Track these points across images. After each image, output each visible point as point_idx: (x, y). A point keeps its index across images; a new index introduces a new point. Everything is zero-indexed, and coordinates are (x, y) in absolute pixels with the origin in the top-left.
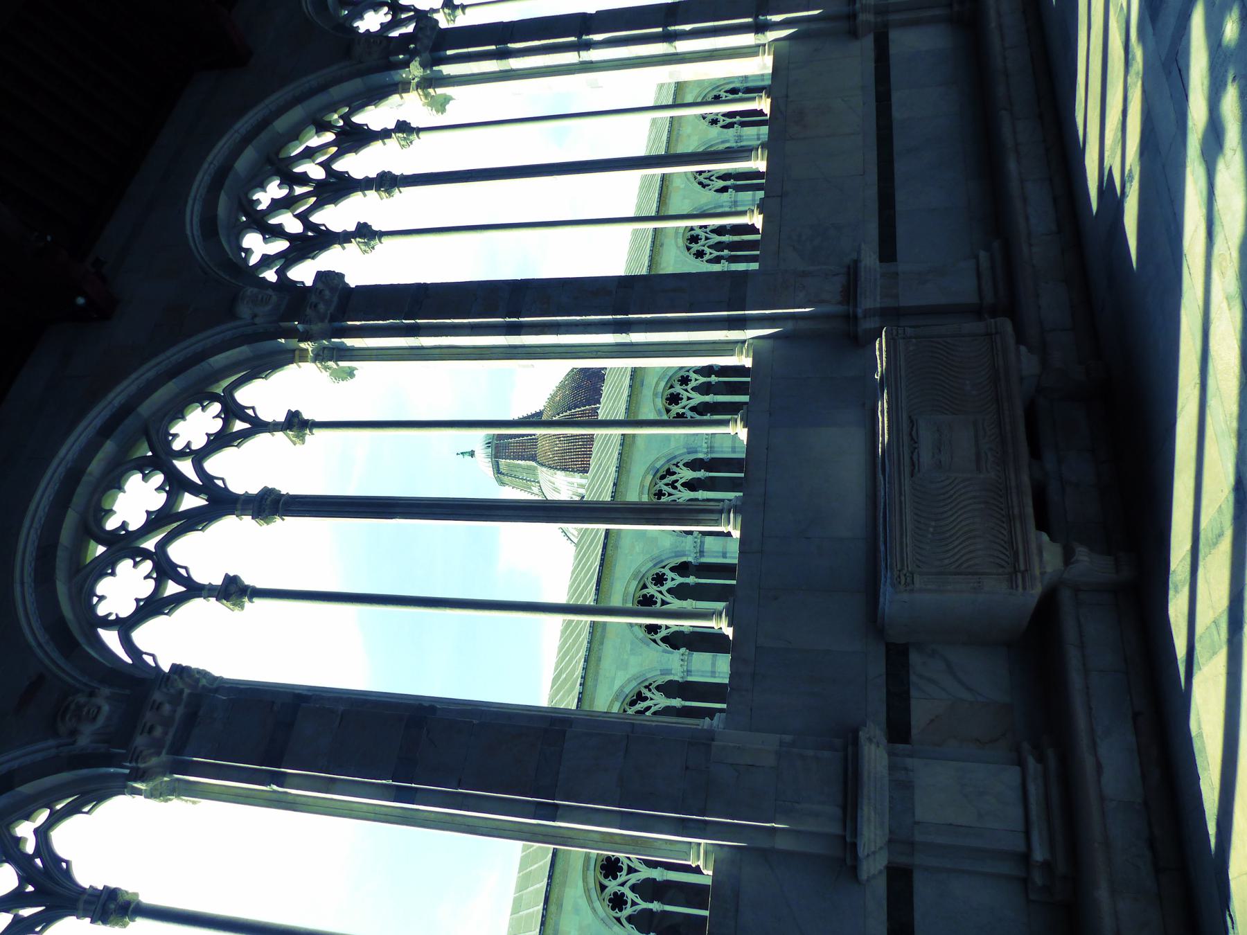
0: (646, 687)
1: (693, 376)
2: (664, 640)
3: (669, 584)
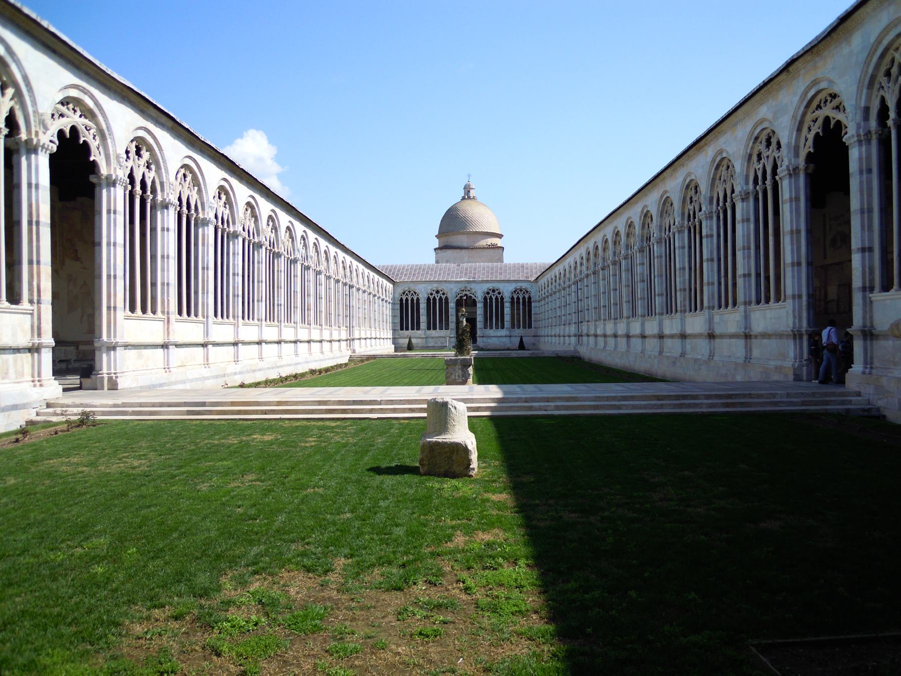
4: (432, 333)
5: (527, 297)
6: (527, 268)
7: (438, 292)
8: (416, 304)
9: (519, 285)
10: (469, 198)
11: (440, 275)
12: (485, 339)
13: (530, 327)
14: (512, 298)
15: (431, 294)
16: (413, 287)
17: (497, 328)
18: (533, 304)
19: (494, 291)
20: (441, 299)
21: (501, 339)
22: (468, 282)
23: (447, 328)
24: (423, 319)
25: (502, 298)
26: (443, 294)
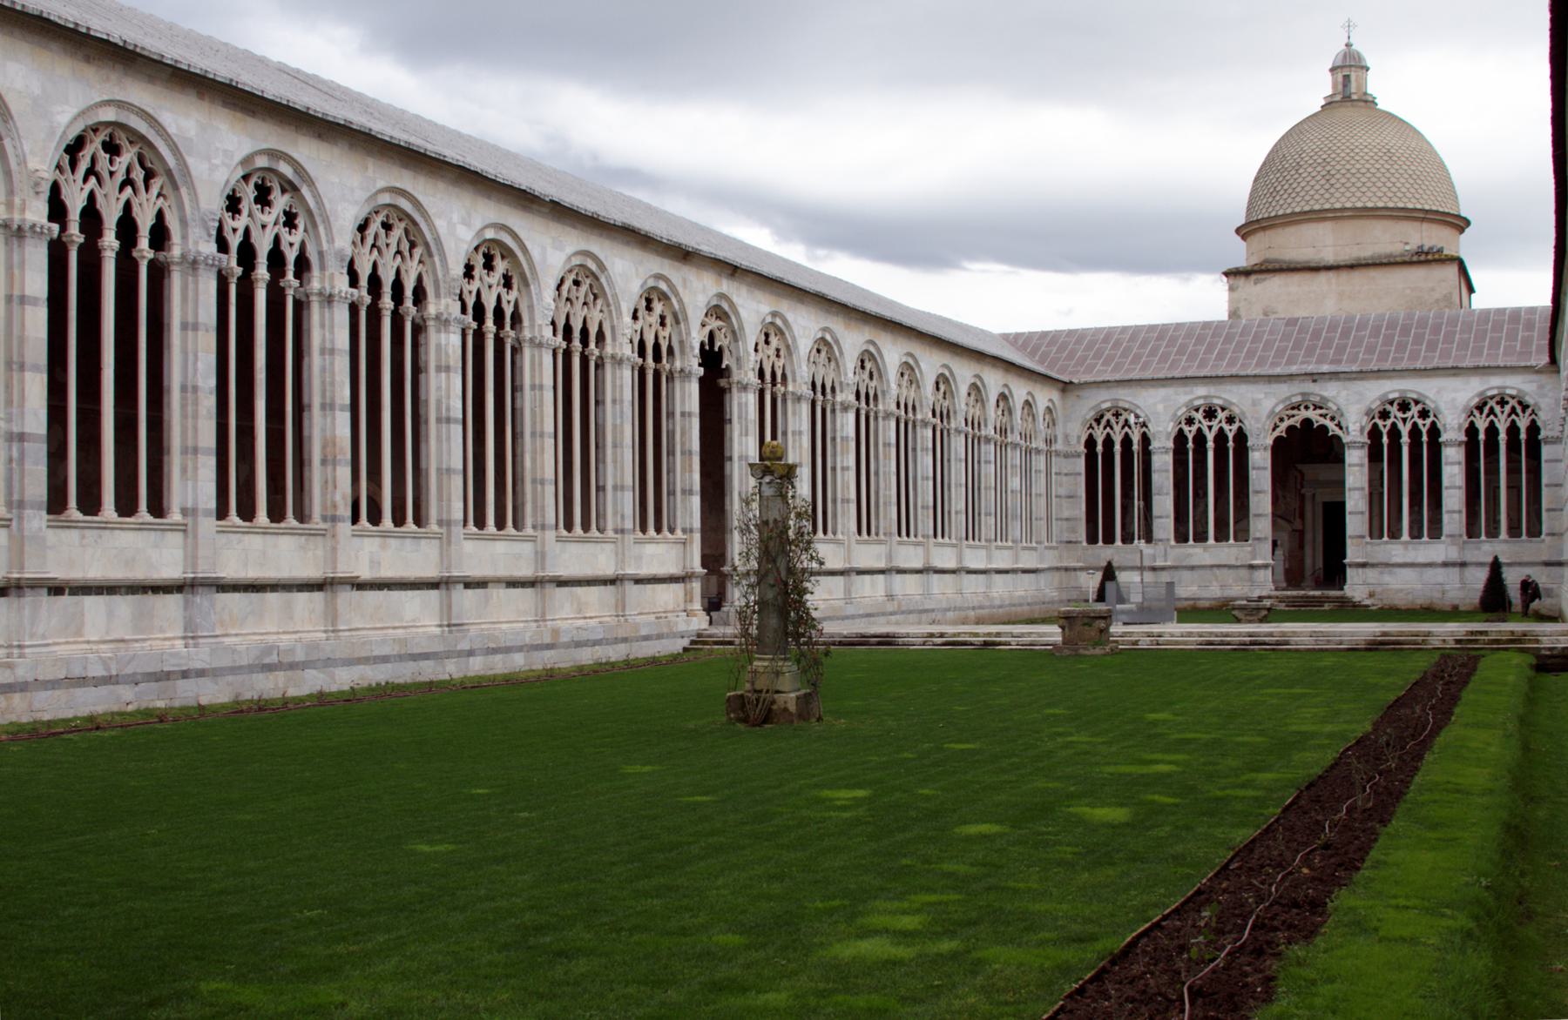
0: (1144, 425)
1: (1428, 422)
2: (1181, 431)
3: (1226, 427)
4: (1196, 553)
5: (1523, 423)
6: (1530, 325)
7: (1210, 414)
8: (1137, 456)
9: (1493, 384)
10: (1347, 98)
11: (1221, 356)
12: (1371, 574)
13: (1534, 531)
14: (1471, 431)
15: (1190, 421)
16: (1125, 396)
17: (1416, 534)
18: (1546, 452)
19: (1404, 406)
20: (1221, 437)
21: (1430, 572)
22: (1314, 377)
23: (1243, 535)
24: (1164, 504)
25: (1434, 432)
26: (1230, 420)
